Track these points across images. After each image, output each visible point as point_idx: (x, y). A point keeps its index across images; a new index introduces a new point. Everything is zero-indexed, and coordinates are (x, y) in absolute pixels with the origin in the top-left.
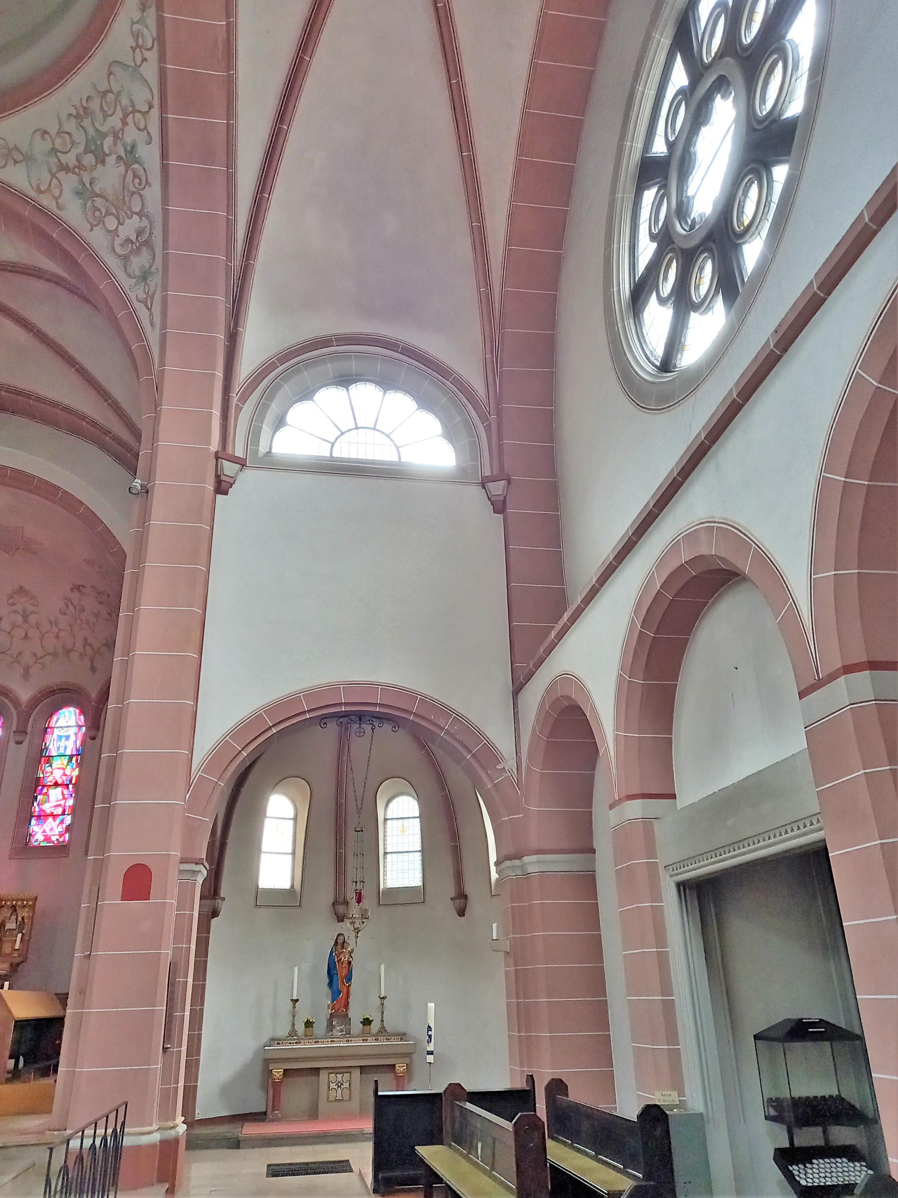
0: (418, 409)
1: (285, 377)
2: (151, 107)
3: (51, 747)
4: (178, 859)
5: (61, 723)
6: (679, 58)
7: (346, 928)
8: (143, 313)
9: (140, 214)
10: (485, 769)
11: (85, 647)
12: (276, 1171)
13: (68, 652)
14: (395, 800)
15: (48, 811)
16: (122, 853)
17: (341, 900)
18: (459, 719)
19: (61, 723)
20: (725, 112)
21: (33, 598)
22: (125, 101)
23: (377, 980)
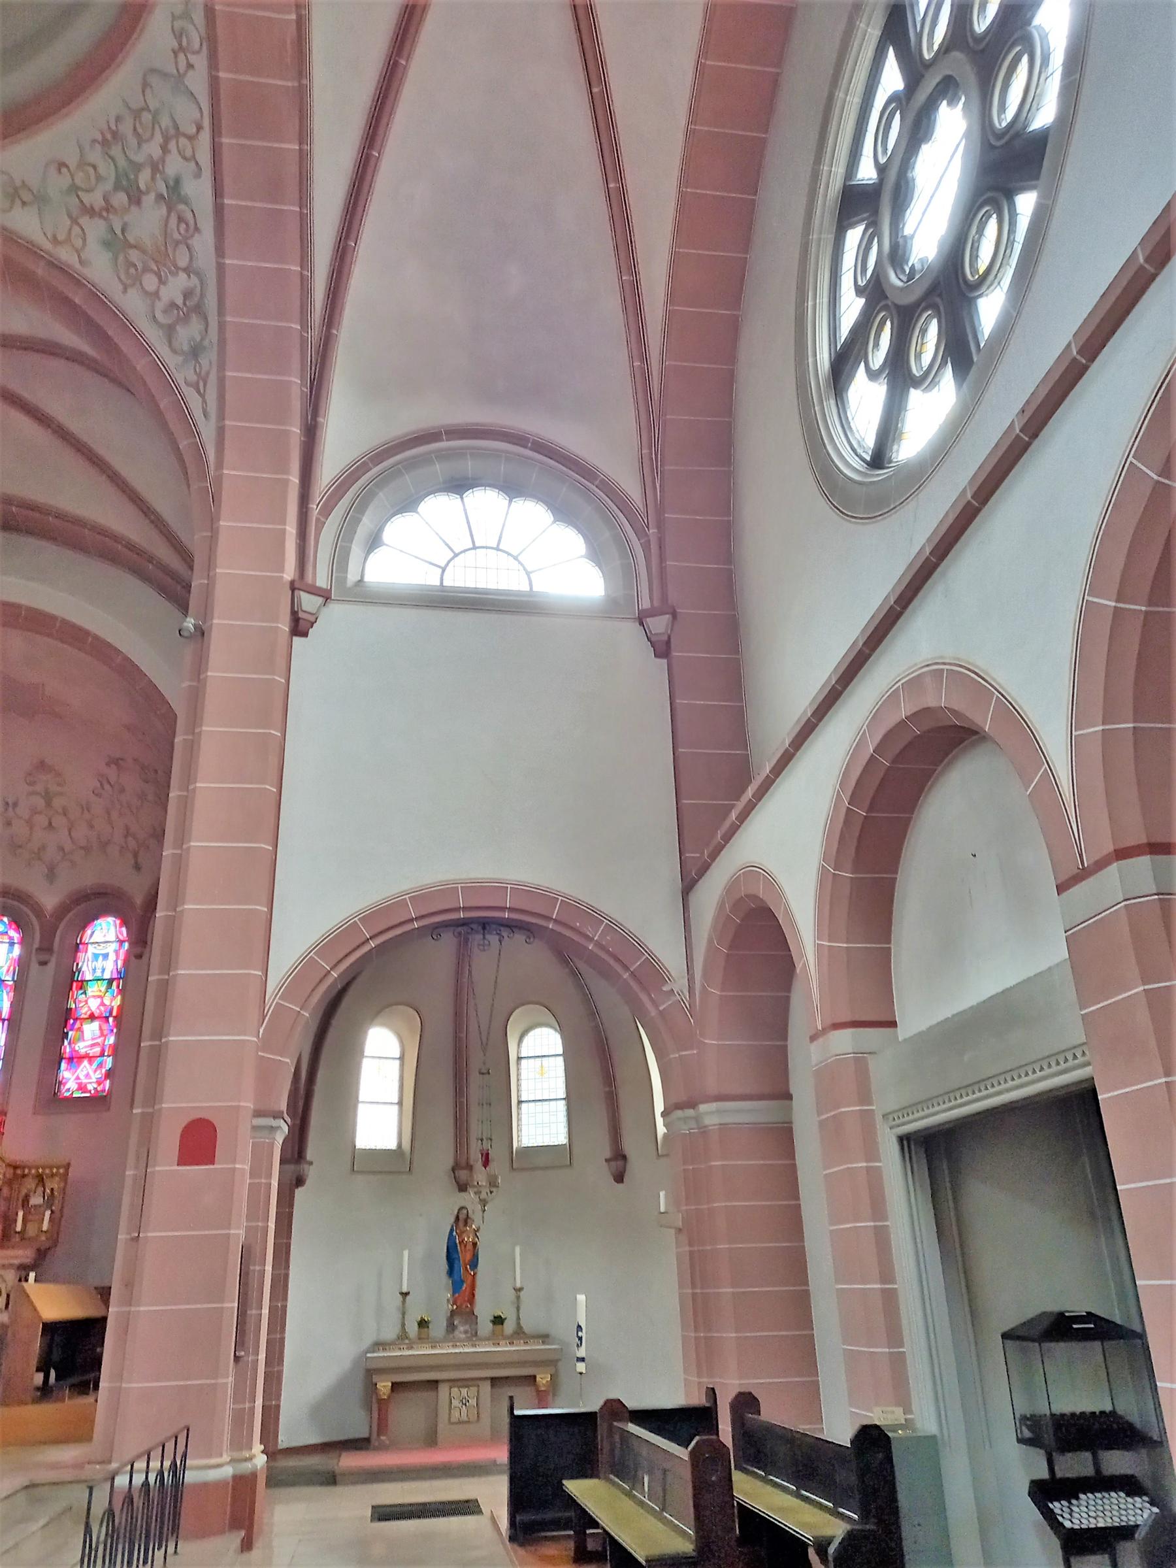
0: (554, 522)
1: (383, 481)
2: (199, 128)
3: (84, 968)
4: (250, 1113)
5: (97, 937)
6: (891, 52)
7: (469, 1199)
8: (194, 401)
9: (187, 270)
10: (644, 988)
11: (126, 837)
12: (383, 1514)
13: (104, 845)
14: (532, 1034)
15: (83, 1051)
16: (179, 1102)
17: (463, 1163)
18: (613, 927)
19: (97, 937)
20: (952, 123)
21: (59, 775)
22: (165, 121)
23: (511, 1268)
